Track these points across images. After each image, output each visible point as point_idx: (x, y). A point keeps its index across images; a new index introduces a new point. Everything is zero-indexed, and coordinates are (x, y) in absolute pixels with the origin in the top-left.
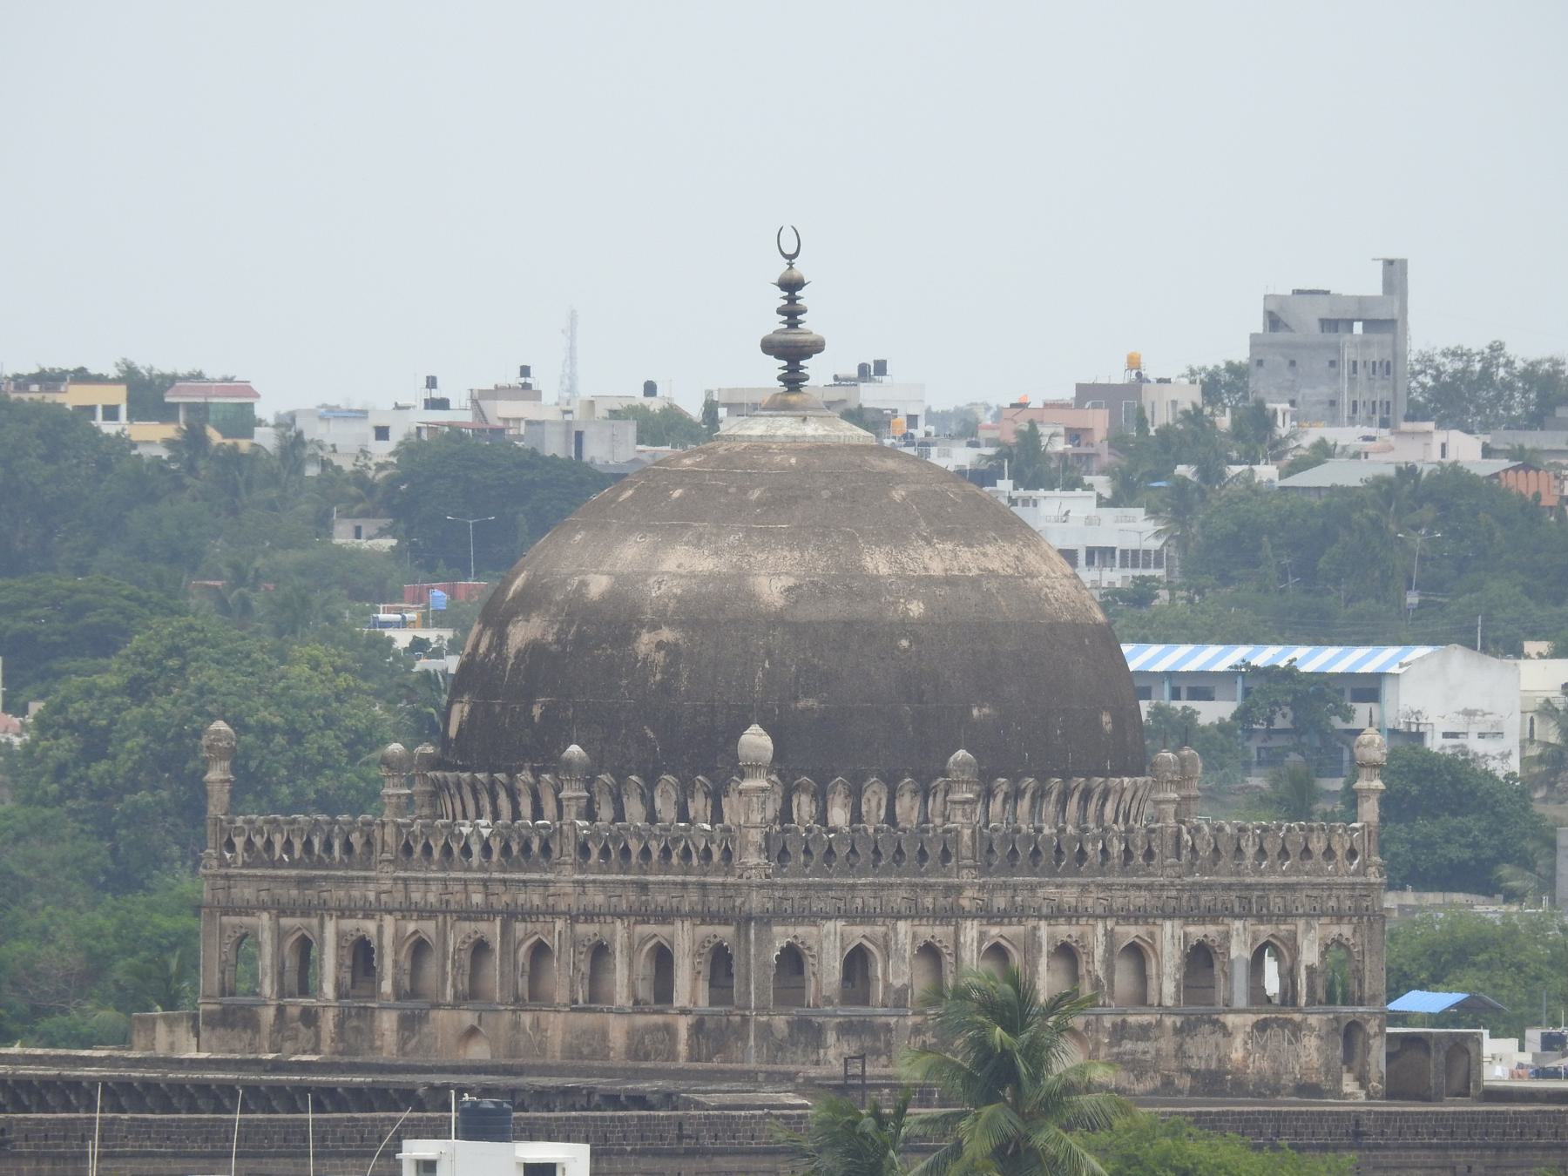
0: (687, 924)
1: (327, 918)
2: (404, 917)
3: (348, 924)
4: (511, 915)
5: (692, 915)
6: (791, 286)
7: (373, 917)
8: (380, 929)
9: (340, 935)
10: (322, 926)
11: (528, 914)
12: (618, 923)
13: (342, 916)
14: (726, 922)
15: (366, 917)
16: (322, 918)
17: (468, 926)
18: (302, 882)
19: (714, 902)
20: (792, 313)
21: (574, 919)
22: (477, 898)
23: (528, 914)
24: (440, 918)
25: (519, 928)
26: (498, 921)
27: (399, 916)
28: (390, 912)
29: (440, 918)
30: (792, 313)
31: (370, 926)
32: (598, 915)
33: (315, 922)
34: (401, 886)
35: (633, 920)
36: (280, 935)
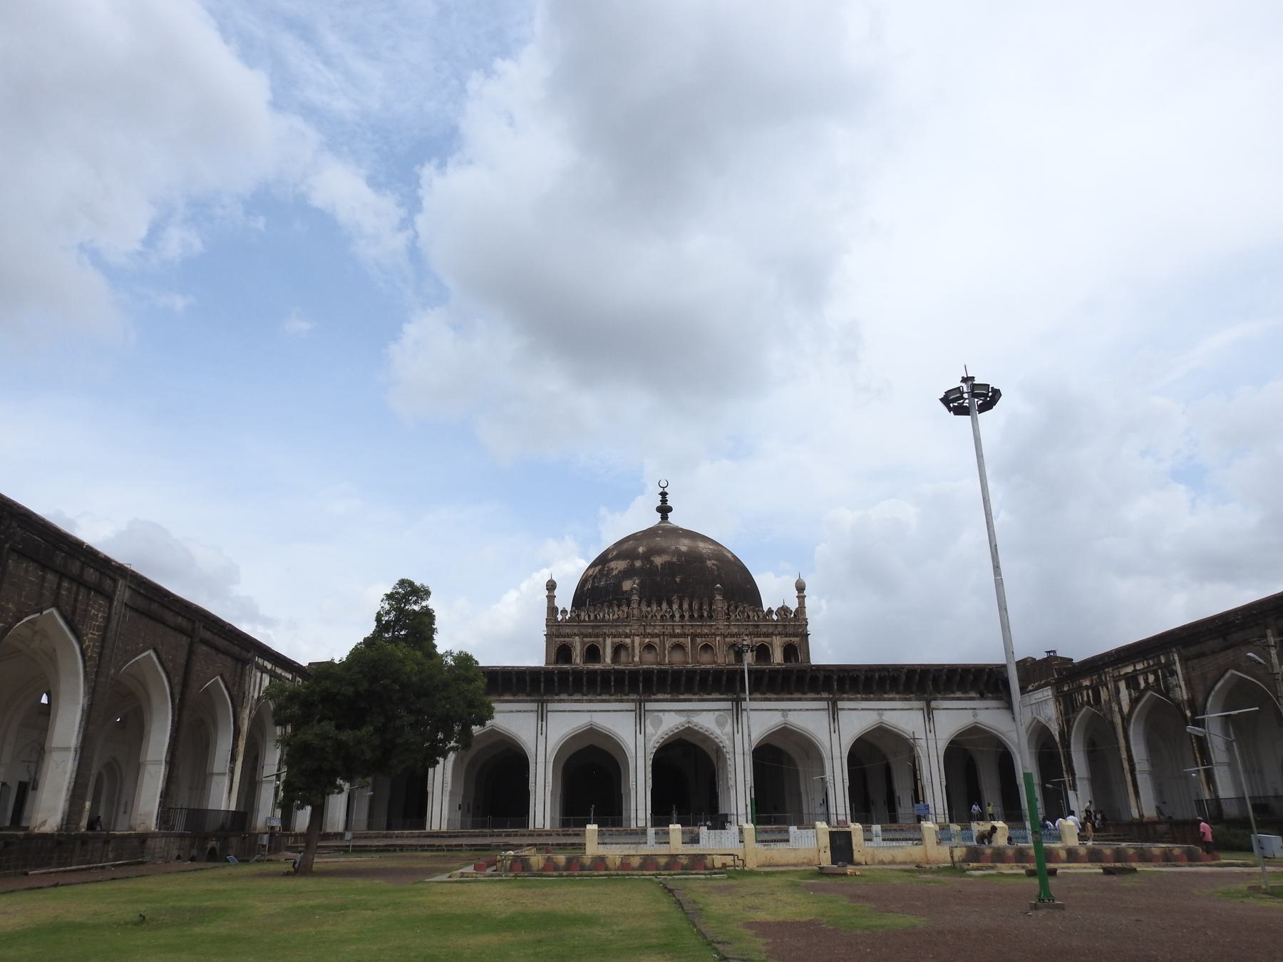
4: (694, 636)
6: (664, 494)
8: (633, 642)
11: (701, 635)
18: (593, 627)
19: (791, 630)
20: (664, 501)
21: (725, 636)
23: (701, 635)
25: (699, 640)
30: (664, 501)
36: (583, 644)
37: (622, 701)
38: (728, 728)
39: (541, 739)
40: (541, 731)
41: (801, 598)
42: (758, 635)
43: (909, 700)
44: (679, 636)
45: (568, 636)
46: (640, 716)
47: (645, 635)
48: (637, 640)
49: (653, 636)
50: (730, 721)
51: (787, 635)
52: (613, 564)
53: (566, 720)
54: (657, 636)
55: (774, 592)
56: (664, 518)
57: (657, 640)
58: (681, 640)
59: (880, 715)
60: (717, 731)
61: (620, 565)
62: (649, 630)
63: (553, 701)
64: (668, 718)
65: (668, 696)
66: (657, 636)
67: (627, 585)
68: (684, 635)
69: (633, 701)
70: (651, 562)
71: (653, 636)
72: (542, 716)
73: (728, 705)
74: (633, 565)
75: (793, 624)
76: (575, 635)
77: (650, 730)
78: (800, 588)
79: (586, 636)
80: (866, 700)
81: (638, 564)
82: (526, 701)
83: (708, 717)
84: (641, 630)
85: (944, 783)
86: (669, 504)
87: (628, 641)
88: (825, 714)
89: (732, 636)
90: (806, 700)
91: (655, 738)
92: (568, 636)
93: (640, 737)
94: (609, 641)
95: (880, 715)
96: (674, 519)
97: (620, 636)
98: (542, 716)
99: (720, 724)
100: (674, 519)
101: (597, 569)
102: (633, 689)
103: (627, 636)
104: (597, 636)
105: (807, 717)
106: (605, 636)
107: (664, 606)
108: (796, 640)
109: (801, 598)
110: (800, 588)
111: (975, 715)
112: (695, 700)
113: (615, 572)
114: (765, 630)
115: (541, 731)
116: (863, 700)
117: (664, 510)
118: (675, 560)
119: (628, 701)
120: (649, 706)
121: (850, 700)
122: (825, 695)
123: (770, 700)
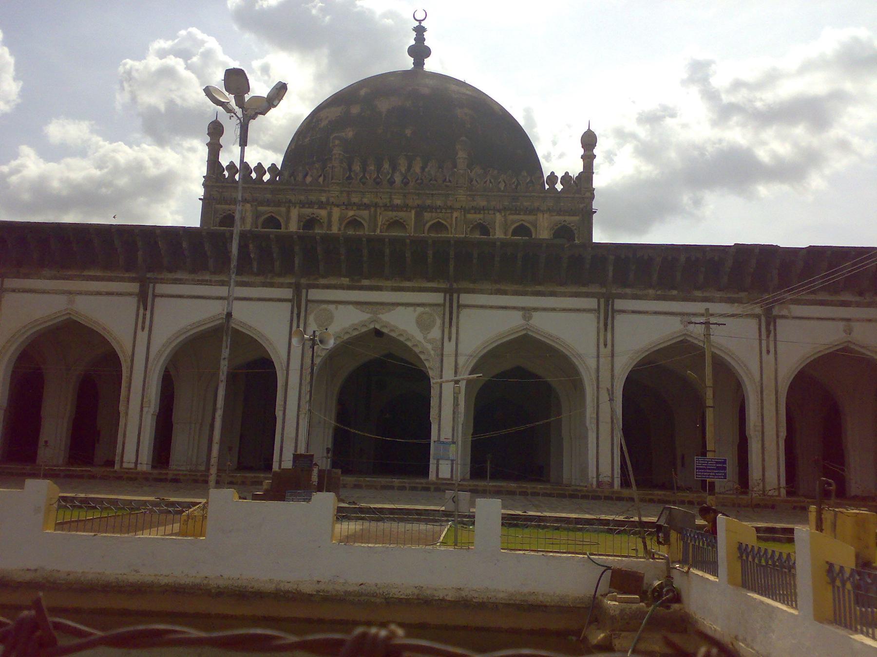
1: (292, 209)
2: (347, 209)
3: (308, 211)
4: (421, 209)
5: (549, 210)
6: (420, 31)
7: (325, 208)
8: (330, 215)
9: (300, 217)
10: (288, 212)
11: (431, 209)
12: (498, 214)
13: (303, 207)
15: (320, 208)
16: (289, 207)
17: (391, 214)
22: (397, 201)
24: (373, 209)
25: (427, 215)
26: (413, 212)
27: (343, 207)
28: (338, 206)
29: (373, 209)
33: (283, 209)
34: (345, 194)
35: (508, 212)
37: (272, 285)
38: (435, 333)
39: (142, 336)
41: (588, 158)
42: (517, 211)
43: (739, 301)
44: (396, 208)
47: (348, 205)
48: (336, 212)
50: (439, 322)
51: (560, 212)
54: (367, 207)
55: (558, 159)
56: (419, 62)
57: (365, 213)
58: (402, 214)
60: (418, 335)
61: (336, 112)
62: (355, 199)
63: (162, 281)
64: (345, 313)
65: (345, 281)
66: (367, 207)
68: (405, 207)
69: (289, 286)
72: (144, 299)
73: (437, 298)
78: (589, 141)
79: (261, 204)
81: (355, 110)
82: (122, 280)
83: (405, 315)
85: (783, 434)
87: (323, 213)
88: (592, 317)
89: (477, 210)
90: (564, 295)
94: (294, 213)
96: (431, 65)
97: (311, 204)
99: (424, 325)
100: (431, 65)
103: (322, 205)
104: (279, 204)
105: (565, 323)
106: (290, 204)
108: (572, 220)
109: (588, 158)
110: (589, 141)
111: (849, 331)
113: (323, 124)
116: (658, 298)
117: (420, 52)
120: (315, 294)
121: (635, 297)
122: (595, 289)
123: (505, 293)
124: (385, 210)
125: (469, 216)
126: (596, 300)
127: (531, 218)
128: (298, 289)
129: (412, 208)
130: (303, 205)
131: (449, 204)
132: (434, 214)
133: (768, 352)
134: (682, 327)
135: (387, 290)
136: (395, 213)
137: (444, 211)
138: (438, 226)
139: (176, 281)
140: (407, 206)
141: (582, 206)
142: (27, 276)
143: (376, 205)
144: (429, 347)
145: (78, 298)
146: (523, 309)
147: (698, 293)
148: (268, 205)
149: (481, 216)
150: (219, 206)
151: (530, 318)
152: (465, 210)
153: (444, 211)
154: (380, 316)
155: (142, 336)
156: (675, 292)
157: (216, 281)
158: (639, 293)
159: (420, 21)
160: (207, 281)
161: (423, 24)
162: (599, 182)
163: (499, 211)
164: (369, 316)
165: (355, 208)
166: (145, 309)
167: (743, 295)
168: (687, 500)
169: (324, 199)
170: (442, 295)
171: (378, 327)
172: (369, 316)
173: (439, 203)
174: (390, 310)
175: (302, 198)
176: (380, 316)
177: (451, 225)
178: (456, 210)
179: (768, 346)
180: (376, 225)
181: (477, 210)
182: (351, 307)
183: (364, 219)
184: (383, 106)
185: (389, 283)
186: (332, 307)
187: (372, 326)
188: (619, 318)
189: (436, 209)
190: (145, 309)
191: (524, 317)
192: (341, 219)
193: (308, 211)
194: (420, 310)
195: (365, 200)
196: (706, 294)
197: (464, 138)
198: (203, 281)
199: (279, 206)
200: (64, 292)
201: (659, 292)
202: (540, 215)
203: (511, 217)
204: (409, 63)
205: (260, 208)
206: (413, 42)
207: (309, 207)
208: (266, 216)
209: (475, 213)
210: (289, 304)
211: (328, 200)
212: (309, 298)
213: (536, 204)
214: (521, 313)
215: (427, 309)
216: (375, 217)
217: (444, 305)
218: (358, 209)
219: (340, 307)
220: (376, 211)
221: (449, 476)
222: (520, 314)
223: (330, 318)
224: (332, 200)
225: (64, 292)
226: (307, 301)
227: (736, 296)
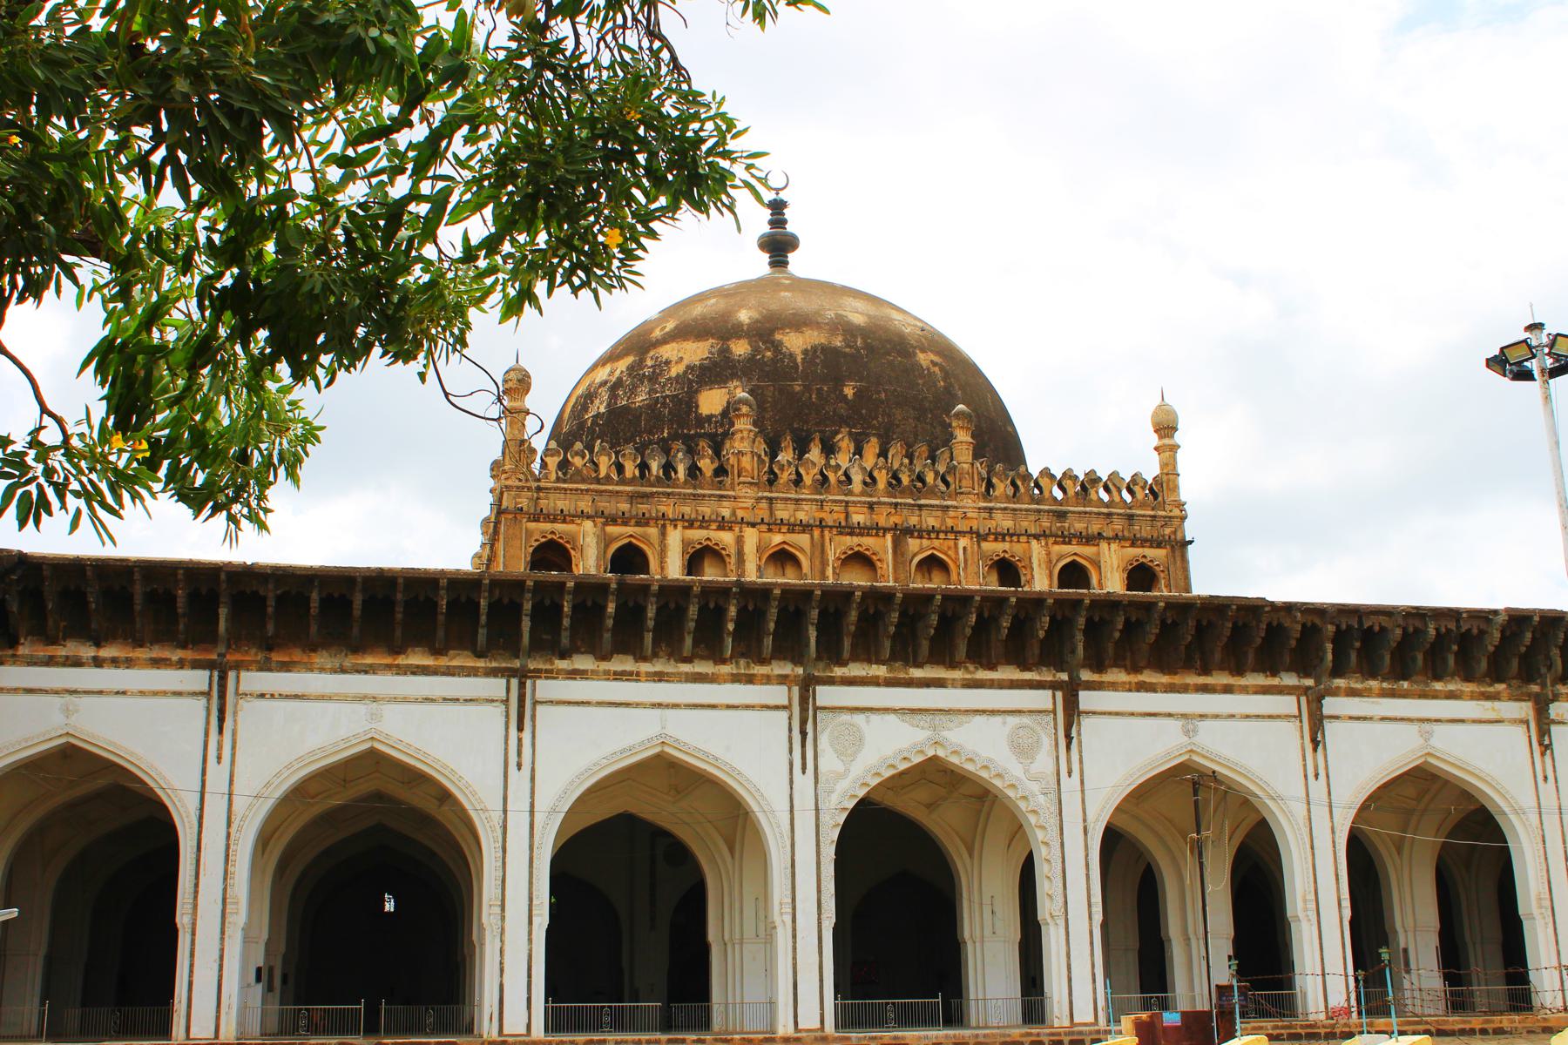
0: (1113, 546)
1: (670, 529)
2: (770, 530)
3: (697, 535)
4: (902, 533)
7: (731, 529)
8: (740, 541)
9: (686, 543)
10: (663, 534)
11: (920, 533)
12: (1034, 542)
14: (1159, 546)
16: (664, 526)
17: (850, 541)
18: (633, 498)
19: (1145, 530)
20: (778, 221)
21: (981, 537)
22: (858, 518)
23: (920, 533)
24: (816, 533)
25: (913, 544)
26: (889, 537)
27: (764, 528)
28: (753, 525)
29: (816, 533)
30: (778, 221)
31: (726, 538)
32: (1012, 535)
33: (653, 531)
34: (764, 505)
35: (1051, 540)
36: (606, 540)
37: (750, 680)
38: (1044, 762)
39: (520, 781)
40: (517, 758)
42: (1066, 539)
44: (862, 531)
45: (564, 517)
46: (806, 713)
47: (773, 525)
48: (751, 537)
49: (794, 527)
50: (1047, 742)
51: (1134, 542)
52: (668, 351)
53: (594, 728)
54: (805, 527)
57: (803, 539)
58: (868, 542)
59: (1426, 736)
62: (783, 513)
63: (551, 675)
64: (881, 729)
65: (880, 671)
66: (805, 527)
67: (711, 402)
68: (876, 530)
69: (783, 680)
70: (777, 347)
71: (794, 527)
74: (725, 351)
75: (1153, 511)
76: (583, 515)
77: (829, 761)
79: (613, 520)
80: (1392, 694)
81: (740, 349)
82: (472, 672)
83: (986, 727)
84: (763, 512)
86: (790, 228)
87: (726, 538)
88: (1291, 728)
89: (1000, 536)
90: (1244, 690)
91: (843, 785)
92: (564, 517)
93: (804, 783)
94: (675, 537)
95: (1426, 736)
97: (704, 523)
98: (522, 715)
99: (1024, 751)
101: (622, 365)
102: (790, 647)
103: (723, 525)
104: (643, 521)
106: (663, 522)
107: (815, 454)
112: (954, 684)
113: (675, 371)
114: (1079, 526)
115: (517, 758)
116: (1384, 694)
117: (779, 246)
118: (838, 342)
119: (767, 680)
122: (1290, 679)
123: (1150, 688)
124: (841, 533)
125: (985, 546)
126: (1294, 698)
127: (1088, 550)
128: (807, 686)
129: (885, 530)
130: (691, 524)
131: (950, 522)
132: (925, 542)
133: (1316, 776)
134: (1421, 741)
135: (954, 687)
136: (856, 540)
137: (942, 536)
138: (932, 564)
139: (574, 674)
140: (878, 528)
141: (1167, 531)
142: (286, 667)
143: (821, 525)
144: (1035, 788)
145: (390, 710)
146: (1184, 716)
147: (1438, 686)
148: (625, 523)
149: (1006, 546)
150: (532, 525)
151: (1195, 731)
152: (981, 537)
153: (942, 536)
154: (945, 733)
155: (520, 781)
156: (1405, 684)
157: (648, 674)
158: (1359, 686)
159: (777, 191)
160: (631, 673)
161: (783, 196)
162: (1190, 488)
163: (1037, 537)
164: (927, 733)
165: (784, 529)
166: (520, 728)
167: (1501, 687)
168: (1478, 1027)
169: (726, 513)
170: (1049, 693)
171: (941, 753)
172: (927, 733)
173: (931, 521)
174: (961, 724)
175: (687, 510)
176: (945, 733)
177: (956, 561)
178: (963, 533)
179: (1544, 771)
180: (824, 563)
181: (1000, 536)
182: (892, 717)
183: (801, 550)
184: (795, 343)
185: (957, 674)
186: (859, 719)
187: (930, 753)
188: (1086, 722)
189: (929, 533)
190: (520, 728)
191: (1187, 733)
192: (760, 549)
193: (697, 535)
194: (1013, 720)
195: (801, 516)
196: (1451, 687)
197: (961, 407)
198: (623, 673)
199: (647, 524)
200: (361, 698)
201: (1385, 685)
202: (1104, 545)
203: (1056, 548)
204: (759, 264)
205: (610, 529)
206: (766, 229)
207: (701, 527)
208: (620, 544)
209: (996, 540)
210: (784, 715)
211: (734, 513)
212: (818, 704)
213: (1095, 528)
214: (1179, 723)
215: (1026, 720)
216: (823, 545)
217: (1054, 712)
218: (793, 531)
219: (875, 718)
220: (822, 536)
221: (1091, 1019)
222: (1175, 725)
223: (859, 741)
224: (740, 514)
225: (361, 698)
226: (816, 709)
227: (1491, 689)
